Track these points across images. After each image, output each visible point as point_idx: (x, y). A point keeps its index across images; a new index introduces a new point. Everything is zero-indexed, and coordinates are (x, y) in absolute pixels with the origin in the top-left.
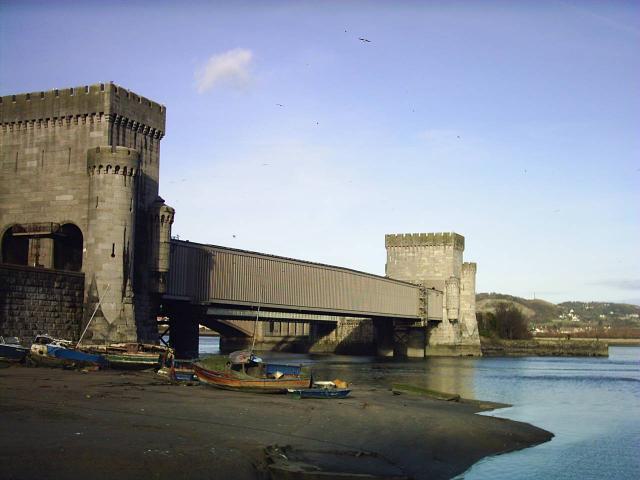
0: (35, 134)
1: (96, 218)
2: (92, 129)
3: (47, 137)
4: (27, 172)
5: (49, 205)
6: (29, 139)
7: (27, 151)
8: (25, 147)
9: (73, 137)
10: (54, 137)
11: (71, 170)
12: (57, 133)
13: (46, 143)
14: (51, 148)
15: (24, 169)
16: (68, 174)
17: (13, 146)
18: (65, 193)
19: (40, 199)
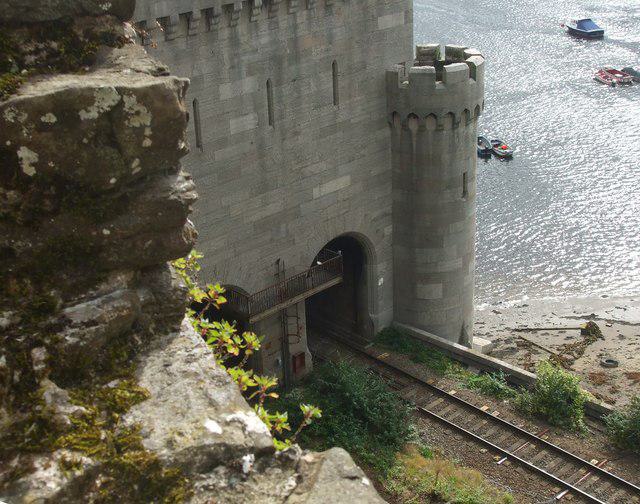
0: (243, 39)
3: (274, 42)
7: (226, 91)
8: (218, 79)
9: (339, 34)
10: (295, 41)
12: (302, 31)
13: (277, 60)
15: (222, 143)
18: (334, 174)
19: (273, 209)
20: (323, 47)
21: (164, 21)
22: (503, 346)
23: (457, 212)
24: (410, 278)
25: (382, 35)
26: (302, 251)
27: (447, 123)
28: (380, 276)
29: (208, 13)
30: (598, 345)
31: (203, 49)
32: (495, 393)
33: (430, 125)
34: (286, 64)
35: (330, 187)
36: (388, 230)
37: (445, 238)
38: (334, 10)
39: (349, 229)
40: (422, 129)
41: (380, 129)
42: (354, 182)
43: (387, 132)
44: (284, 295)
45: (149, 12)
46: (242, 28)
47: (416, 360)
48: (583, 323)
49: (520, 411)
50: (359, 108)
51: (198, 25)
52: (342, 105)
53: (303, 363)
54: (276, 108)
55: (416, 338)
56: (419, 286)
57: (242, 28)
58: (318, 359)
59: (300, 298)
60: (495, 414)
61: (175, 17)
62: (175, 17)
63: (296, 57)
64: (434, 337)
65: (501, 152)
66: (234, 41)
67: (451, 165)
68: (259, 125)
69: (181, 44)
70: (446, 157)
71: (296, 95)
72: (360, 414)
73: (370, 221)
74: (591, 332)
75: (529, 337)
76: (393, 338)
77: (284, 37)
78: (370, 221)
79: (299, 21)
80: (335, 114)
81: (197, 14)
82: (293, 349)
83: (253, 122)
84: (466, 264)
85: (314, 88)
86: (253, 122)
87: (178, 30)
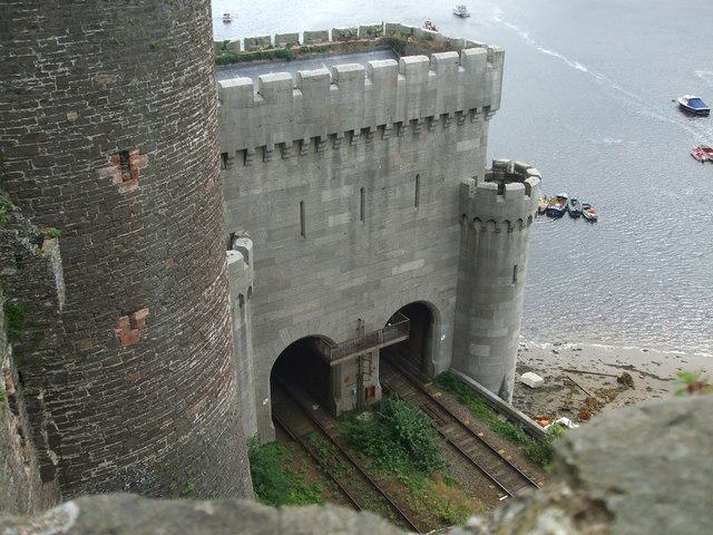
3: (370, 160)
7: (327, 196)
8: (322, 186)
9: (423, 154)
10: (386, 160)
11: (421, 216)
12: (393, 152)
13: (370, 174)
14: (380, 182)
15: (322, 233)
16: (413, 224)
17: (289, 191)
18: (410, 258)
19: (358, 282)
21: (282, 146)
22: (553, 383)
23: (507, 295)
24: (465, 340)
25: (460, 154)
26: (379, 314)
27: (504, 228)
28: (443, 334)
29: (317, 140)
30: (629, 393)
31: (311, 165)
32: (513, 438)
33: (490, 228)
34: (377, 177)
35: (405, 268)
36: (453, 300)
37: (495, 313)
38: (421, 136)
39: (420, 299)
40: (483, 230)
42: (426, 264)
43: (458, 227)
44: (359, 347)
45: (269, 139)
46: (344, 150)
47: (462, 402)
48: (620, 372)
49: (528, 457)
50: (435, 209)
51: (309, 148)
53: (373, 394)
54: (367, 208)
55: (464, 383)
57: (344, 150)
58: (386, 392)
59: (375, 349)
60: (508, 458)
61: (289, 143)
62: (289, 143)
63: (386, 172)
64: (478, 385)
65: (587, 214)
66: (337, 159)
68: (352, 220)
69: (294, 161)
70: (501, 253)
72: (406, 443)
73: (437, 292)
74: (626, 382)
75: (575, 378)
76: (449, 382)
77: (377, 157)
78: (437, 292)
79: (391, 145)
80: (415, 213)
81: (307, 140)
82: (366, 384)
84: (510, 333)
87: (292, 152)
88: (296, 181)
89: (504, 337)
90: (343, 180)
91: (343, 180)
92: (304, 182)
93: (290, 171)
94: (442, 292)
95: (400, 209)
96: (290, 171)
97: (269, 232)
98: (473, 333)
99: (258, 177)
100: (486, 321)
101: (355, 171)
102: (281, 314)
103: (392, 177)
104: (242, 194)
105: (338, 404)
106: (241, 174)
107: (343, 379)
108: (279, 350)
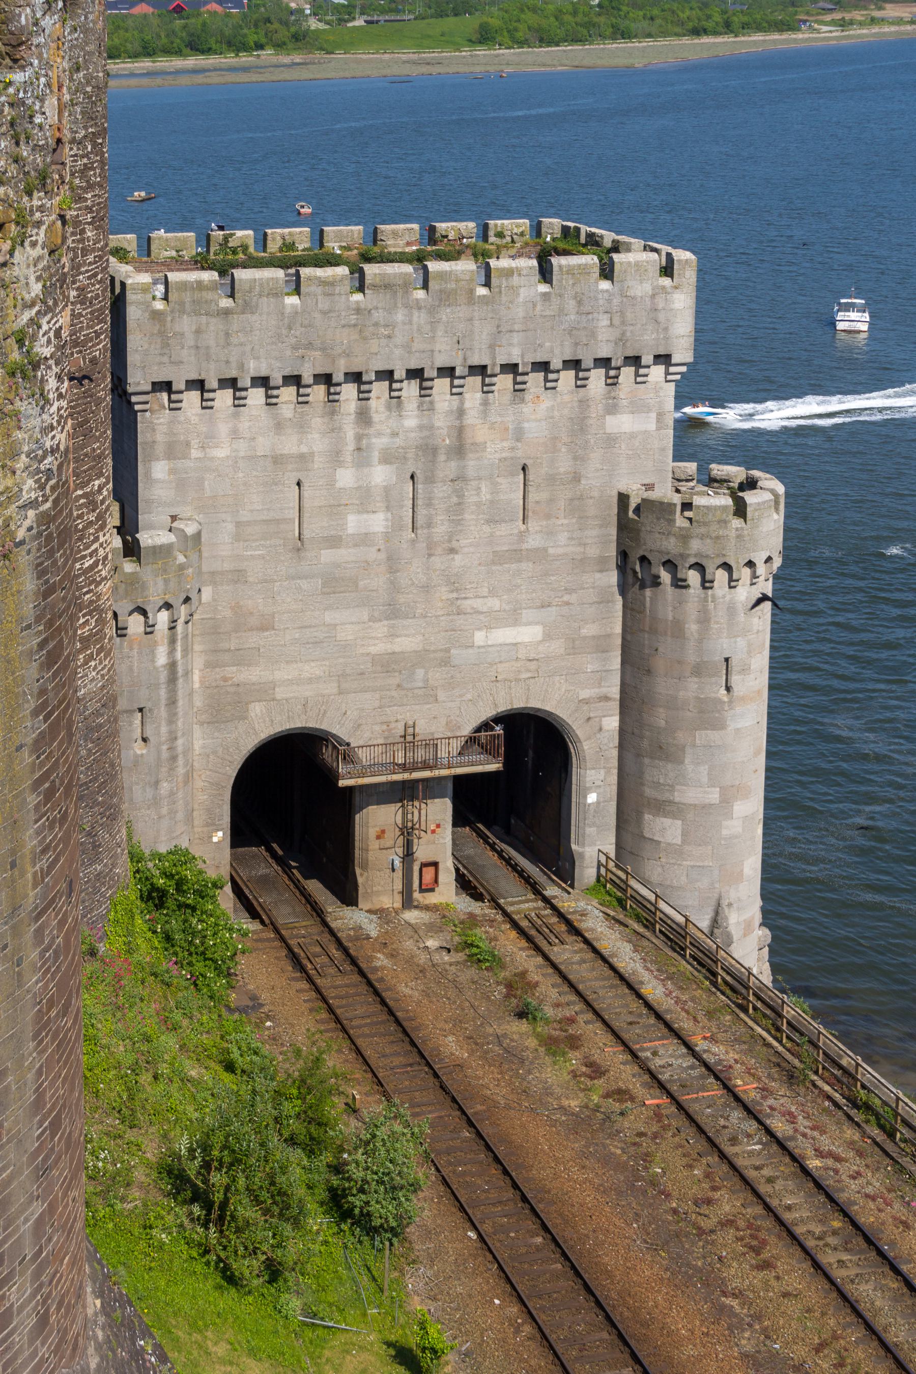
0: (376, 418)
1: (723, 727)
2: (612, 409)
4: (344, 554)
5: (445, 662)
6: (350, 431)
7: (346, 477)
8: (335, 458)
10: (460, 431)
11: (534, 542)
12: (472, 418)
13: (429, 450)
14: (447, 468)
15: (334, 542)
16: (517, 555)
17: (278, 460)
18: (513, 618)
19: (407, 643)
20: (506, 444)
25: (611, 441)
31: (317, 422)
34: (442, 458)
35: (505, 635)
36: (612, 723)
37: (688, 750)
38: (528, 396)
41: (601, 571)
42: (548, 637)
52: (533, 525)
54: (422, 512)
56: (647, 817)
66: (364, 417)
67: (700, 641)
68: (396, 527)
71: (455, 500)
77: (442, 422)
80: (522, 536)
83: (384, 523)
85: (485, 494)
86: (384, 523)
88: (290, 445)
89: (705, 808)
90: (376, 455)
91: (376, 455)
92: (304, 449)
93: (279, 426)
94: (586, 701)
95: (488, 522)
96: (279, 426)
97: (238, 524)
98: (649, 792)
99: (223, 429)
100: (669, 766)
101: (398, 441)
102: (253, 675)
103: (472, 464)
104: (195, 453)
105: (360, 880)
106: (195, 419)
107: (372, 832)
108: (249, 744)
